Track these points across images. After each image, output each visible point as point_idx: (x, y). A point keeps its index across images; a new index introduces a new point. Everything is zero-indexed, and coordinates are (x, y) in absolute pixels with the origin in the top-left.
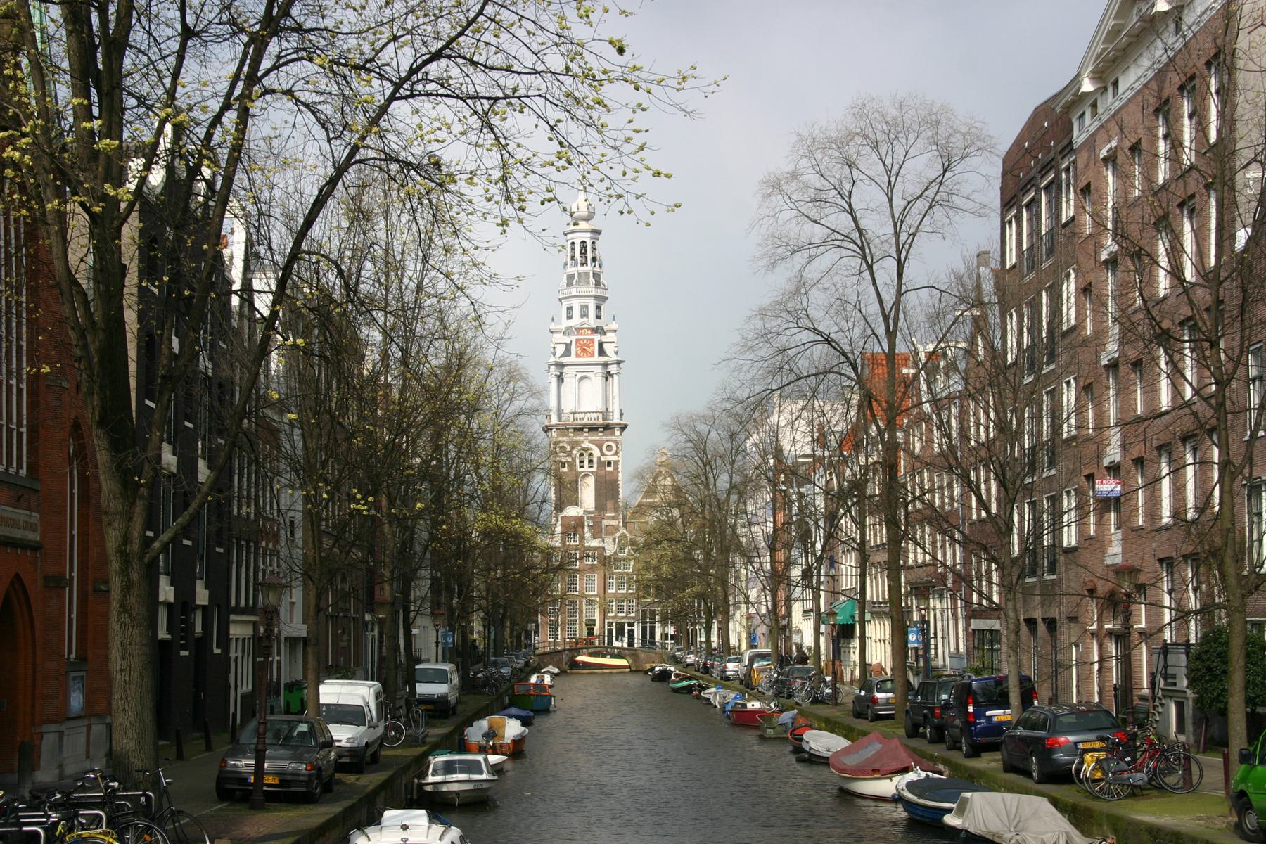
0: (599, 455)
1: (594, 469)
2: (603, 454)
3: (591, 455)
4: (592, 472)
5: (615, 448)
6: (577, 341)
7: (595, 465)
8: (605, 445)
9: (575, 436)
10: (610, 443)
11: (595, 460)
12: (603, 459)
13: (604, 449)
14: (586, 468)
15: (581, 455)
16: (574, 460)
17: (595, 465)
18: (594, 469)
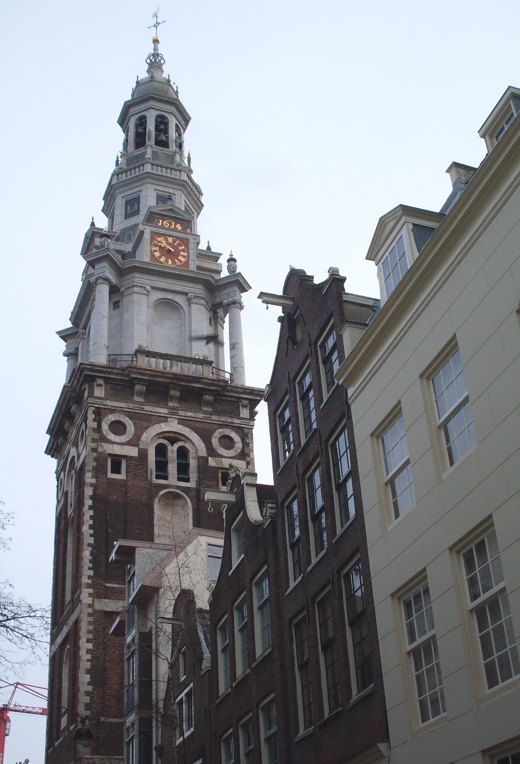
0: (203, 451)
1: (192, 484)
2: (212, 452)
3: (183, 453)
4: (186, 490)
5: (237, 438)
6: (154, 234)
7: (193, 475)
8: (217, 434)
9: (148, 402)
10: (228, 432)
11: (193, 463)
12: (212, 462)
13: (215, 441)
14: (173, 479)
15: (161, 450)
16: (143, 455)
17: (193, 475)
18: (192, 484)
